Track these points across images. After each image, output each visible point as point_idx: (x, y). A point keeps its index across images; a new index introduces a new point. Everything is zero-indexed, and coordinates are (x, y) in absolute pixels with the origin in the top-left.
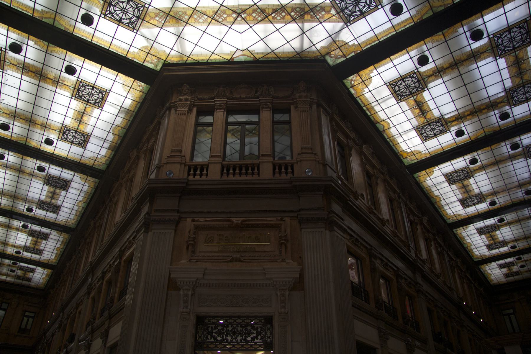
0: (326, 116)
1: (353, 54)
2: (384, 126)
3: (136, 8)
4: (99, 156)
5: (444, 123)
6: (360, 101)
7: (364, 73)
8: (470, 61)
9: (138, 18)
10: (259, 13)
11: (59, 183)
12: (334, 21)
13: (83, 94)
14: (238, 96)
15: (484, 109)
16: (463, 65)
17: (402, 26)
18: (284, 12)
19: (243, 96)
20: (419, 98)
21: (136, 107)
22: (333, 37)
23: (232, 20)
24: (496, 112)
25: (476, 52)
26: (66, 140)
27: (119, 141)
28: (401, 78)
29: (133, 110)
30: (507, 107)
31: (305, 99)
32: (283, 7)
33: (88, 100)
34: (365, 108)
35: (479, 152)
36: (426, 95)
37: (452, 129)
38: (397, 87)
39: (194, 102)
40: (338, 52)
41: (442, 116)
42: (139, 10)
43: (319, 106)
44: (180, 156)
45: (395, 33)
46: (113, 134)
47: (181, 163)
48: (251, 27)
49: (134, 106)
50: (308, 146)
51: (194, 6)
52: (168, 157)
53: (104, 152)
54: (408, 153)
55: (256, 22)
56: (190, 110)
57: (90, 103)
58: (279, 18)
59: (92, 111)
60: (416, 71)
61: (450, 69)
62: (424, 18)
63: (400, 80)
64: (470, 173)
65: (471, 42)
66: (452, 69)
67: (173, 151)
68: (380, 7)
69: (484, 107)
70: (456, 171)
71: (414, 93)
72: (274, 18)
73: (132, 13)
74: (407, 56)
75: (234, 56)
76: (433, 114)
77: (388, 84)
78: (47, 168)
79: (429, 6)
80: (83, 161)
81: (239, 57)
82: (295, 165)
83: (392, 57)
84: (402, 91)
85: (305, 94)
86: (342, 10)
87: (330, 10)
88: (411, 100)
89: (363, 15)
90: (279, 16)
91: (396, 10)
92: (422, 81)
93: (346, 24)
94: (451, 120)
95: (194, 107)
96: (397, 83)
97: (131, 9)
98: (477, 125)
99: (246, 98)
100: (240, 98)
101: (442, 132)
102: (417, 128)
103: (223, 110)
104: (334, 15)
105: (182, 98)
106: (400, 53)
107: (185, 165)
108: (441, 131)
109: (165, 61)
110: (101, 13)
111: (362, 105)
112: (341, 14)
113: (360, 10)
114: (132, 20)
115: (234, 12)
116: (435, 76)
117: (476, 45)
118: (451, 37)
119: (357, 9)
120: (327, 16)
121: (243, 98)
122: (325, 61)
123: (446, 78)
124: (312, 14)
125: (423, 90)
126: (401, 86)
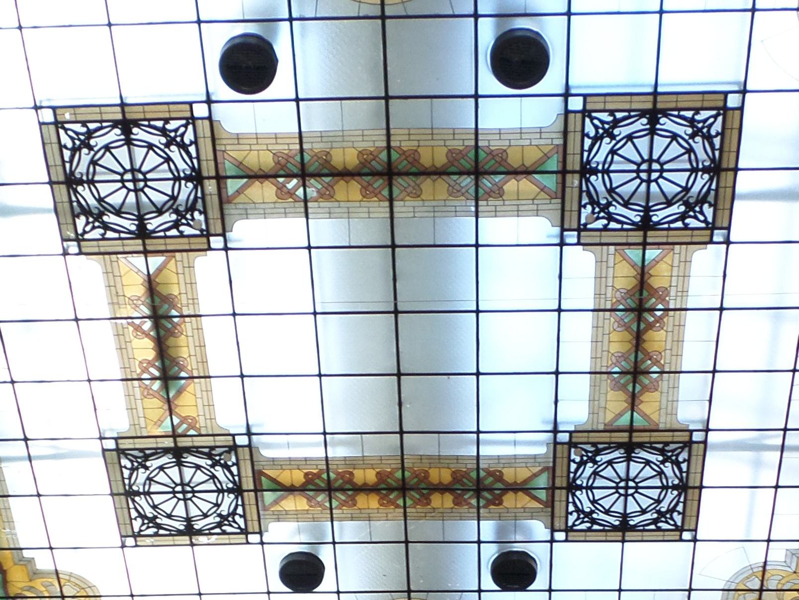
8: (456, 192)
15: (442, 489)
24: (488, 529)
30: (539, 529)
38: (85, 156)
41: (249, 434)
54: (35, 574)
65: (490, 83)
66: (367, 193)
69: (446, 477)
84: (104, 189)
94: (285, 477)
96: (90, 134)
102: (120, 452)
116: (283, 193)
126: (107, 160)
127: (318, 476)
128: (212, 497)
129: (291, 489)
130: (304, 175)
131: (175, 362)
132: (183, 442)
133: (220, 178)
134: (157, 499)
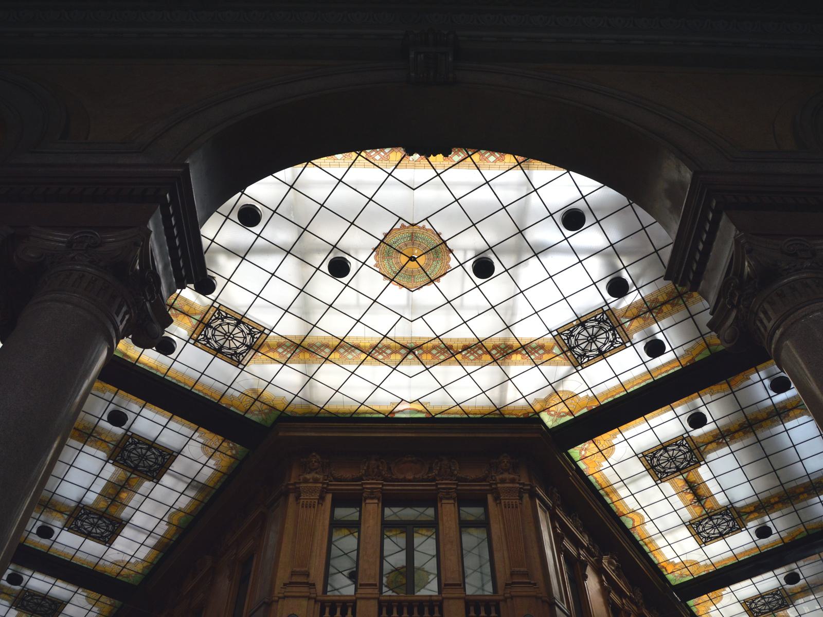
0: (545, 512)
1: (585, 410)
2: (633, 520)
3: (248, 334)
4: (133, 560)
5: (736, 516)
6: (593, 481)
7: (603, 440)
9: (250, 347)
10: (441, 349)
11: (42, 606)
12: (557, 364)
13: (129, 457)
14: (401, 477)
15: (802, 493)
16: (761, 427)
17: (663, 371)
18: (480, 348)
19: (410, 476)
20: (692, 477)
21: (218, 481)
22: (554, 387)
23: (398, 357)
25: (781, 408)
26: (77, 531)
27: (177, 536)
28: (661, 447)
29: (211, 484)
31: (511, 485)
32: (480, 342)
33: (137, 466)
34: (601, 492)
35: (801, 563)
36: (703, 472)
37: (750, 524)
38: (655, 460)
39: (328, 485)
40: (561, 408)
42: (253, 337)
43: (533, 495)
44: (307, 583)
45: (652, 380)
46: (169, 523)
47: (309, 598)
48: (427, 369)
49: (215, 480)
50: (522, 569)
51: (341, 336)
52: (285, 585)
53: (143, 553)
54: (675, 564)
55: (437, 361)
56: (322, 498)
57: (140, 471)
58: (472, 357)
59: (140, 485)
60: (685, 436)
61: (741, 433)
62: (697, 359)
63: (660, 450)
64: (787, 599)
65: (772, 393)
66: (745, 433)
67: (293, 574)
68: (628, 344)
70: (762, 596)
71: (683, 468)
72: (464, 357)
73: (241, 340)
74: (670, 414)
75: (397, 409)
76: (716, 502)
77: (641, 455)
78: (25, 578)
79: (704, 344)
80: (98, 568)
81: (404, 410)
82: (502, 604)
83: (646, 416)
84: (663, 465)
85: (512, 476)
86: (571, 349)
87: (553, 348)
88: (679, 480)
89: (602, 354)
90: (472, 354)
91: (655, 348)
92: (696, 451)
93: (575, 367)
94: (748, 510)
95: (326, 493)
96: (655, 454)
97: (241, 335)
98: (793, 520)
99: (414, 480)
100: (405, 480)
101: (733, 531)
102: (691, 524)
103: (376, 501)
104: (557, 356)
105: (308, 476)
106: (660, 410)
107: (316, 601)
108: (731, 528)
109: (283, 412)
110: (190, 338)
111: (598, 487)
112: (569, 354)
113: (599, 349)
114: (239, 351)
115: (404, 347)
116: (718, 444)
117: (780, 398)
118: (741, 386)
119: (594, 347)
120: (546, 357)
121: (410, 481)
122: (541, 421)
123: (734, 447)
124: (524, 352)
125: (698, 464)
126: (662, 458)
127: (759, 505)
128: (726, 524)
129: (751, 512)
130: (724, 437)
131: (700, 496)
132: (710, 514)
133: (698, 448)
134: (708, 531)
